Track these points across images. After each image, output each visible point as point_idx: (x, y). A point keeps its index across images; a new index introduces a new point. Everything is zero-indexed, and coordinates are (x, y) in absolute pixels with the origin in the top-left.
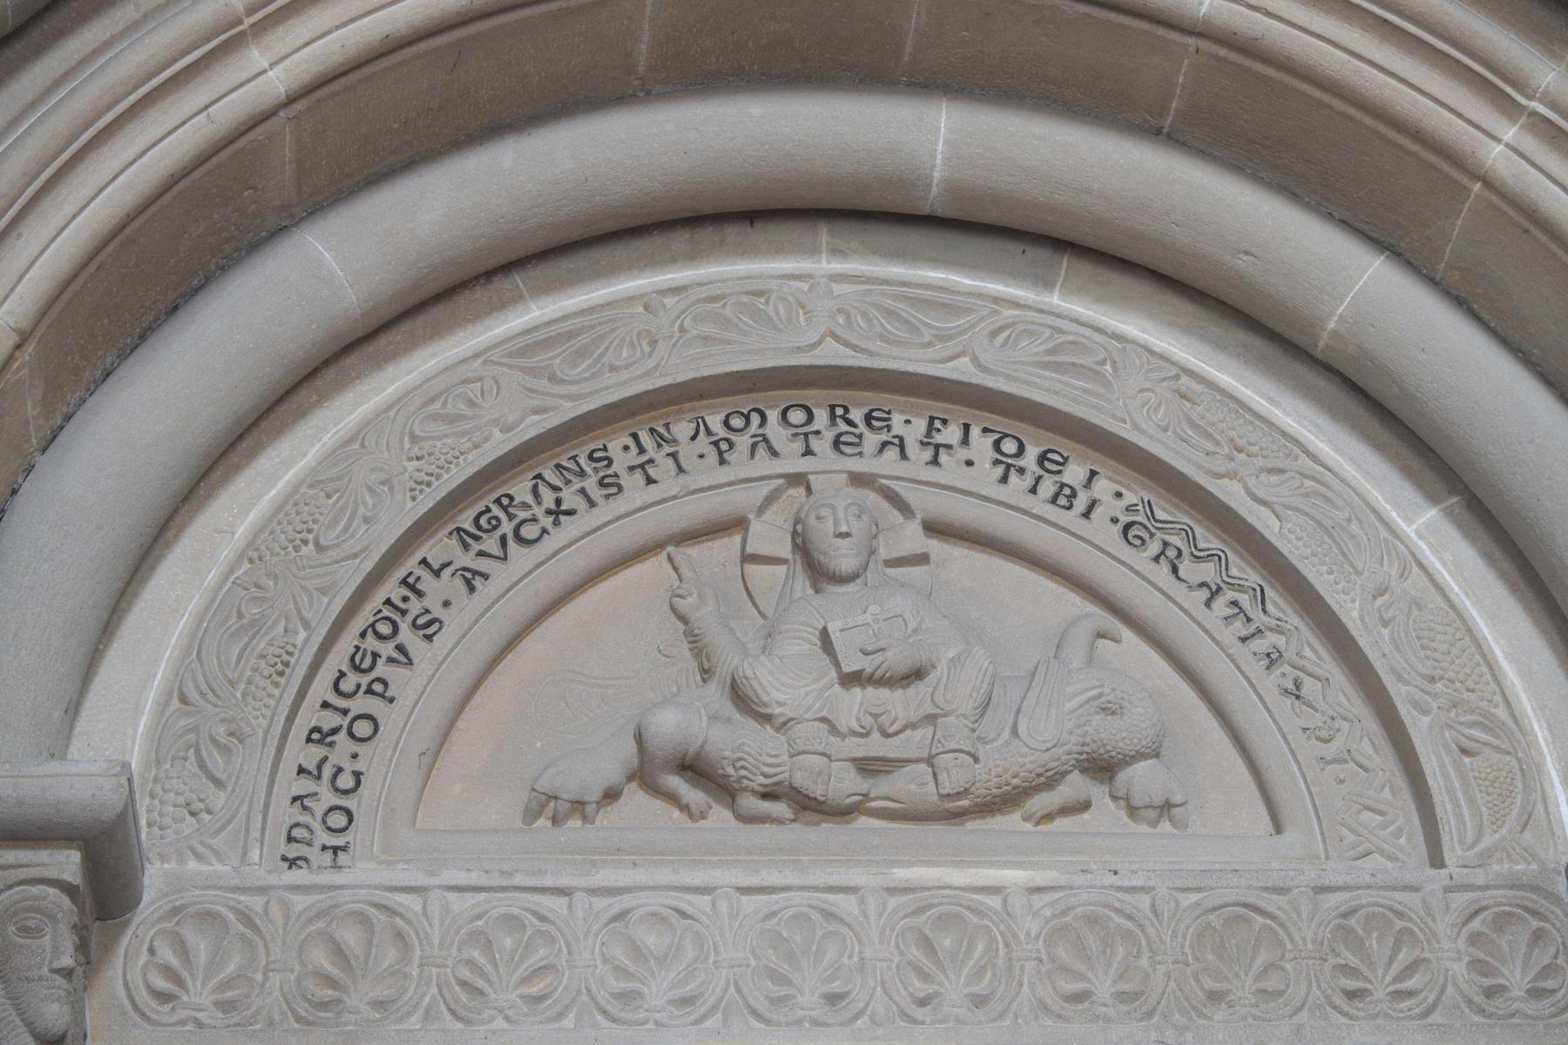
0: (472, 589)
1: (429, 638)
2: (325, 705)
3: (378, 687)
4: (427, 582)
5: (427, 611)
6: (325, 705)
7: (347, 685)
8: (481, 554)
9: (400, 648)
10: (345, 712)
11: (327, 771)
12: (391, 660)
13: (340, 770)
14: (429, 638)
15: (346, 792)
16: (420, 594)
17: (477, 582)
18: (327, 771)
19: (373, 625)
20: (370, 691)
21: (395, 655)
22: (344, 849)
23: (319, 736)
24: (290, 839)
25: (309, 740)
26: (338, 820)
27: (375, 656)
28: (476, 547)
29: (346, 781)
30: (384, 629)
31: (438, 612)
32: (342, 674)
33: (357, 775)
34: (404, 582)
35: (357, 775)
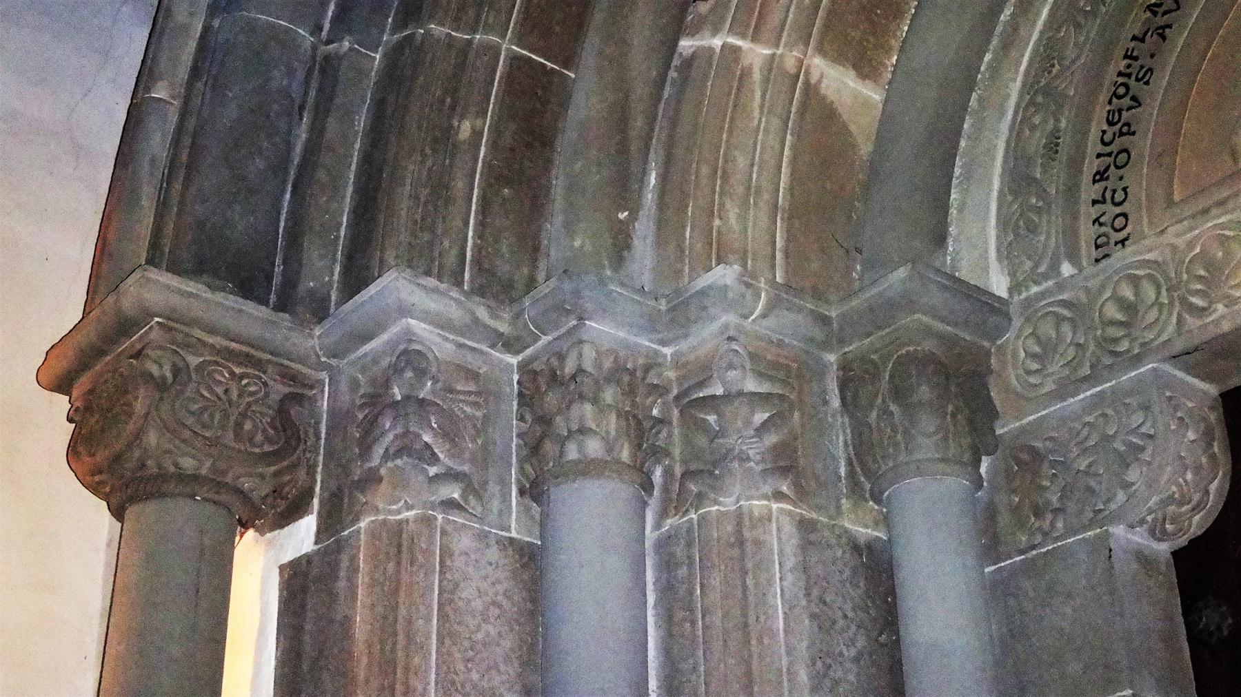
0: (1164, 38)
1: (1147, 83)
2: (1099, 156)
3: (1125, 129)
4: (1140, 49)
5: (1142, 67)
6: (1099, 156)
7: (1107, 138)
8: (1165, 13)
9: (1134, 98)
10: (1109, 155)
11: (1108, 195)
12: (1129, 109)
13: (1114, 191)
14: (1147, 83)
15: (1120, 204)
16: (1136, 59)
17: (1167, 31)
18: (1108, 195)
19: (1115, 94)
20: (1121, 134)
21: (1133, 103)
22: (1127, 239)
23: (1100, 176)
24: (1097, 247)
25: (1095, 181)
26: (1119, 222)
27: (1120, 111)
28: (1161, 10)
29: (1119, 196)
30: (1122, 90)
31: (1148, 62)
32: (1104, 132)
33: (1125, 189)
34: (1126, 57)
35: (1125, 189)
